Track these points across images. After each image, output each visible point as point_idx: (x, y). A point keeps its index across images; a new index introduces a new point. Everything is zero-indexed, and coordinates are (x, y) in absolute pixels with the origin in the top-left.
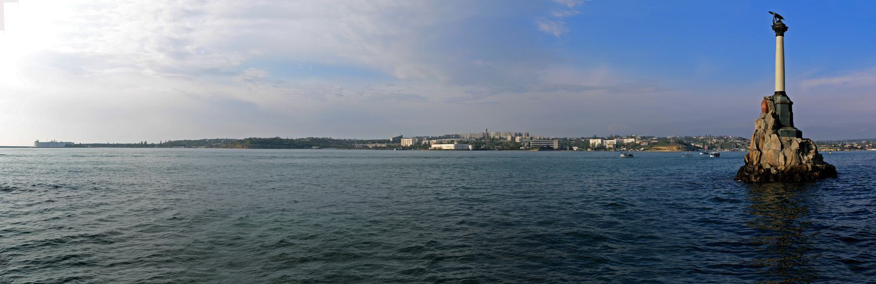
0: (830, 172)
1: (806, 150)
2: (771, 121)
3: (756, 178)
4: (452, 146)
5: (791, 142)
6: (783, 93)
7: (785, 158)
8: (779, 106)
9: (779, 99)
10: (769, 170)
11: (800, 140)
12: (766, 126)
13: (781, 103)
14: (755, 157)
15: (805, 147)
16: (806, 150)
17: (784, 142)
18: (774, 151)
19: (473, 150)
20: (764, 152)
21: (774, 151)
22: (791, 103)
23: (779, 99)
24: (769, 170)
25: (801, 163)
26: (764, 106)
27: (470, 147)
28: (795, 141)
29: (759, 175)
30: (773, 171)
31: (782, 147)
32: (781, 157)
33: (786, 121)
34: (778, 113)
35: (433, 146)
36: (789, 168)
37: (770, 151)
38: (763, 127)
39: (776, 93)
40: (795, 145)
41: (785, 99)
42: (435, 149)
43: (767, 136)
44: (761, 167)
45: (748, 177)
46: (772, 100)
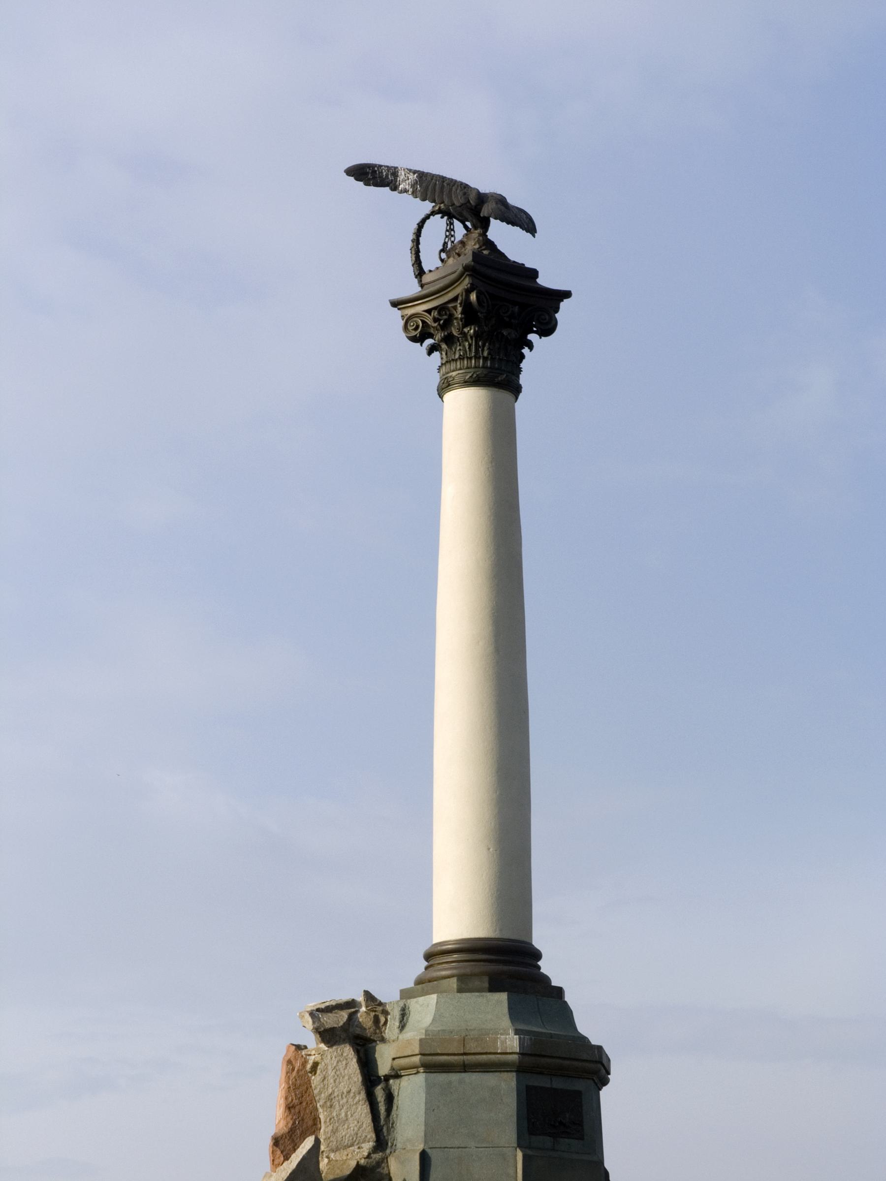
8: (411, 1093)
41: (492, 1018)
46: (352, 1029)
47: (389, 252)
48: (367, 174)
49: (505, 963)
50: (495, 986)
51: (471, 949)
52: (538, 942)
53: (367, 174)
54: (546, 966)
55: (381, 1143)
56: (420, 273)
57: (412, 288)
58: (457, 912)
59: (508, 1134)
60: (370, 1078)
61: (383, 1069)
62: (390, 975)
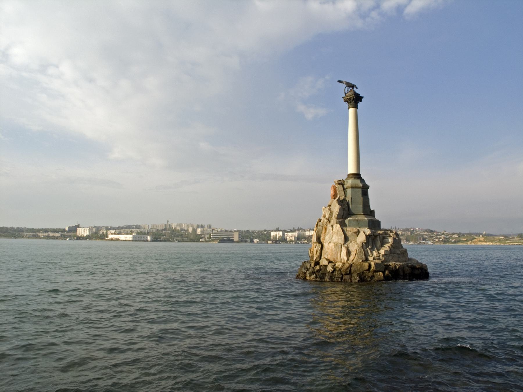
0: (419, 273)
1: (379, 243)
2: (336, 208)
3: (310, 276)
4: (130, 237)
5: (358, 233)
6: (357, 176)
7: (349, 253)
8: (349, 191)
9: (350, 182)
10: (326, 266)
11: (368, 231)
12: (331, 213)
13: (352, 187)
14: (315, 250)
15: (374, 241)
16: (379, 243)
17: (349, 233)
18: (336, 244)
19: (152, 241)
20: (326, 245)
21: (336, 244)
22: (368, 187)
23: (350, 182)
24: (326, 266)
25: (367, 260)
26: (332, 192)
27: (149, 238)
28: (362, 233)
29: (313, 273)
30: (330, 269)
31: (346, 239)
32: (344, 251)
33: (358, 207)
34: (348, 199)
35: (110, 236)
36: (347, 265)
37: (331, 244)
38: (327, 217)
39: (349, 175)
40: (362, 238)
41: (358, 182)
42: (112, 240)
43: (329, 227)
44: (317, 263)
45: (305, 273)
46: (341, 183)
47: (342, 90)
48: (340, 82)
49: (357, 176)
50: (358, 179)
51: (353, 174)
52: (361, 173)
53: (340, 82)
54: (362, 176)
55: (345, 196)
56: (345, 94)
57: (344, 96)
58: (352, 170)
59: (361, 195)
60: (344, 189)
61: (345, 188)
62: (344, 177)
